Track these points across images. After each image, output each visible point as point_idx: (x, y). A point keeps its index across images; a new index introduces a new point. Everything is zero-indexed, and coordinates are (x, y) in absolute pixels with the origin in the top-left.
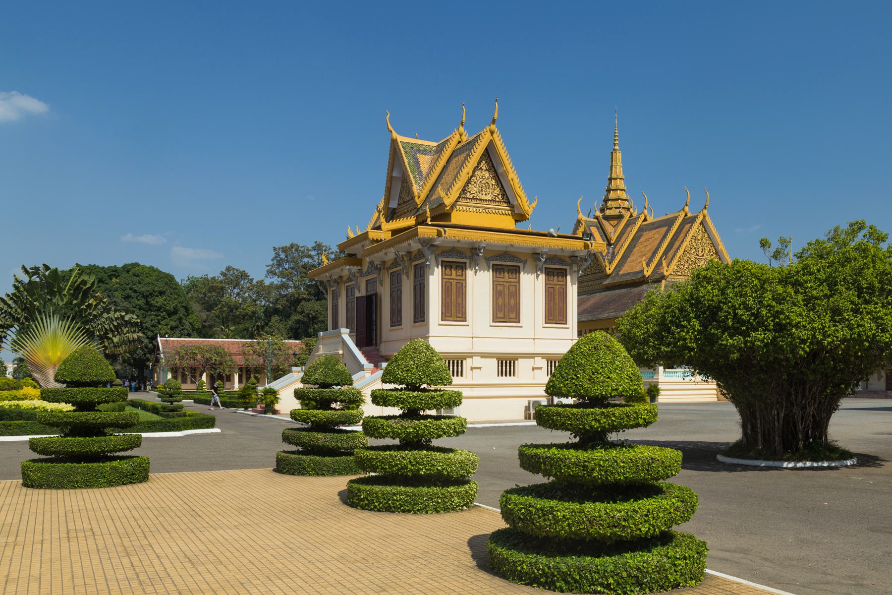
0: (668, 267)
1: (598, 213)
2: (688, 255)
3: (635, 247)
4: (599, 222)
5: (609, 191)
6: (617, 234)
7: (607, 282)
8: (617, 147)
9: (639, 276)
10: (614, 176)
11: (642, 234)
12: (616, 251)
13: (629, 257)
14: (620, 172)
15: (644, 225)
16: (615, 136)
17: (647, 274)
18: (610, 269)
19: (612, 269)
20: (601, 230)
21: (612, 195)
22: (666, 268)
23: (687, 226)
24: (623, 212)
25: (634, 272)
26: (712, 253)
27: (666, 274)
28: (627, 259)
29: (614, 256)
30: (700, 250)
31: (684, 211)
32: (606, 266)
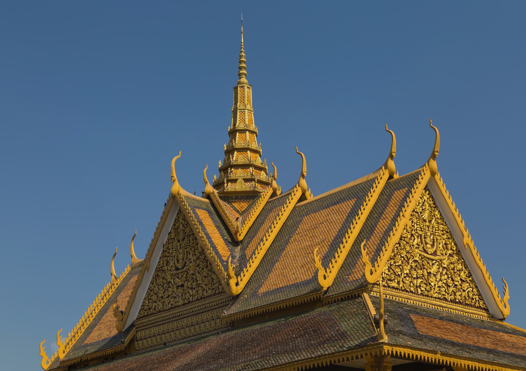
0: (374, 266)
1: (209, 188)
2: (408, 248)
3: (287, 243)
4: (213, 205)
5: (230, 151)
6: (249, 224)
7: (235, 309)
8: (244, 80)
9: (306, 290)
10: (240, 125)
11: (300, 222)
12: (248, 252)
13: (277, 261)
14: (250, 120)
15: (302, 206)
16: (241, 62)
17: (326, 283)
18: (237, 284)
19: (242, 285)
20: (217, 218)
21: (237, 158)
22: (368, 267)
23: (399, 195)
24: (259, 188)
25: (291, 286)
26: (450, 252)
27: (371, 279)
28: (273, 264)
29: (243, 262)
30: (428, 240)
31: (386, 167)
32: (230, 277)
